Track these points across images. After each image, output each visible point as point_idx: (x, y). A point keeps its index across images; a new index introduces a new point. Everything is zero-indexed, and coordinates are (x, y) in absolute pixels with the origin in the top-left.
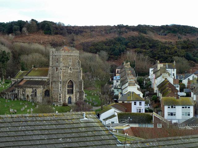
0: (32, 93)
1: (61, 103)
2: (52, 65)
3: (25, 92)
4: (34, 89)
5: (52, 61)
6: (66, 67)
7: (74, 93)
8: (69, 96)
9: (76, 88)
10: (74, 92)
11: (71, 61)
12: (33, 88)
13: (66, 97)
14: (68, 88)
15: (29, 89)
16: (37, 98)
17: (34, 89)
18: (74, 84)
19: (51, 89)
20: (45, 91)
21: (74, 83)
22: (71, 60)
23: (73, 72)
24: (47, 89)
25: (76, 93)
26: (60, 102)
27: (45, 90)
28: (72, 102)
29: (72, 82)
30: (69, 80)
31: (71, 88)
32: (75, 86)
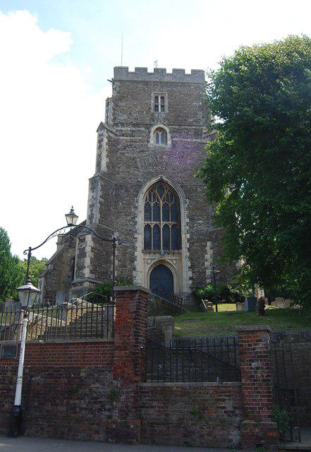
1: (81, 283)
6: (134, 125)
7: (185, 245)
8: (157, 257)
9: (192, 219)
10: (185, 237)
11: (166, 104)
13: (133, 259)
14: (146, 218)
18: (182, 201)
21: (181, 195)
22: (166, 97)
23: (174, 145)
25: (198, 242)
26: (79, 280)
28: (176, 290)
29: (174, 195)
30: (154, 181)
31: (170, 223)
32: (187, 209)
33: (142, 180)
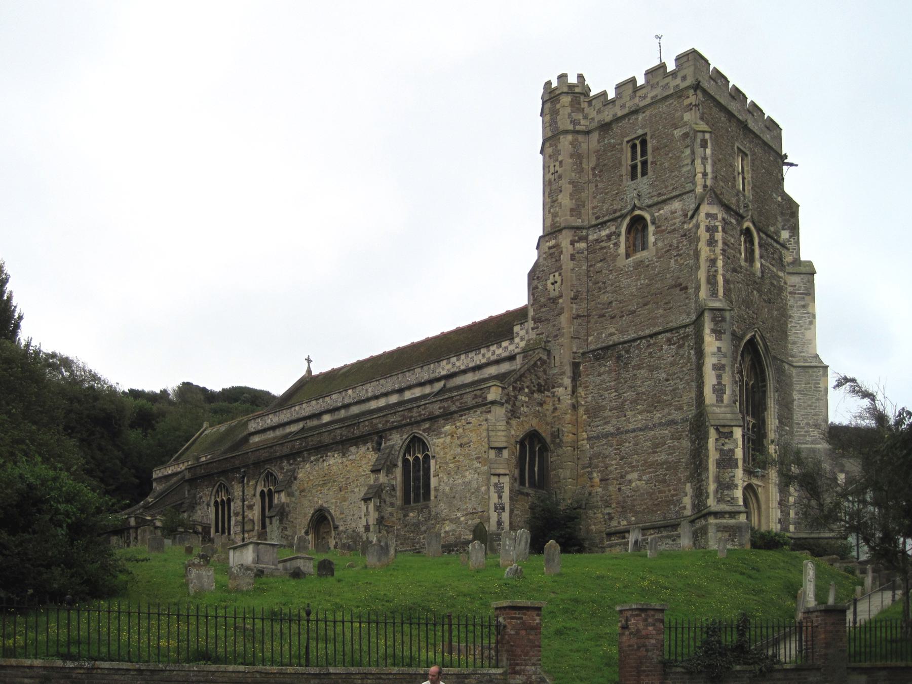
0: (382, 478)
1: (733, 514)
2: (575, 211)
3: (290, 495)
4: (397, 440)
5: (572, 182)
12: (377, 437)
15: (334, 461)
16: (442, 508)
17: (397, 440)
19: (566, 428)
20: (522, 443)
24: (534, 423)
26: (726, 508)
27: (518, 430)
33: (736, 330)
